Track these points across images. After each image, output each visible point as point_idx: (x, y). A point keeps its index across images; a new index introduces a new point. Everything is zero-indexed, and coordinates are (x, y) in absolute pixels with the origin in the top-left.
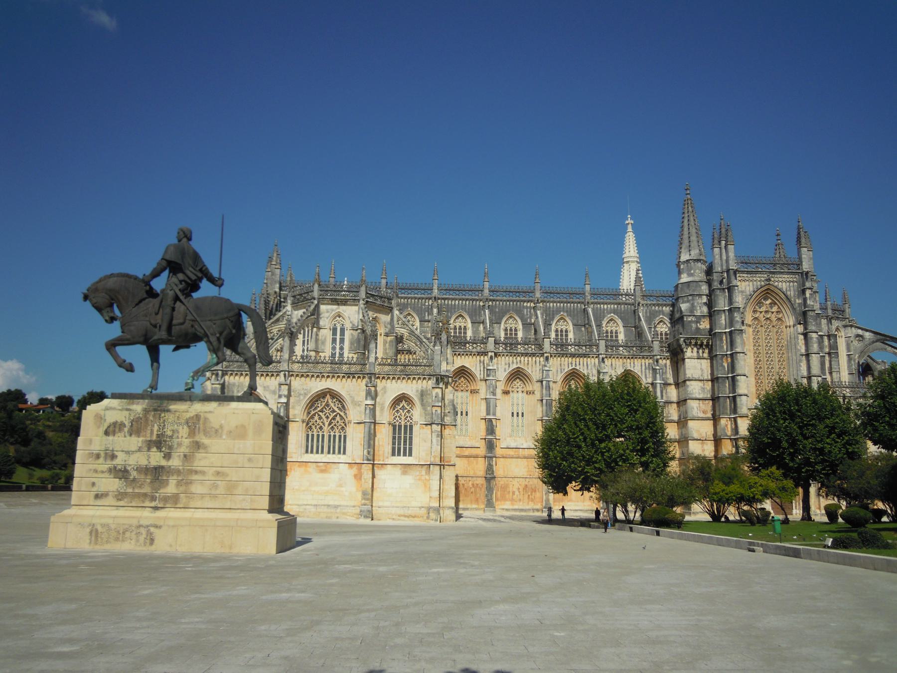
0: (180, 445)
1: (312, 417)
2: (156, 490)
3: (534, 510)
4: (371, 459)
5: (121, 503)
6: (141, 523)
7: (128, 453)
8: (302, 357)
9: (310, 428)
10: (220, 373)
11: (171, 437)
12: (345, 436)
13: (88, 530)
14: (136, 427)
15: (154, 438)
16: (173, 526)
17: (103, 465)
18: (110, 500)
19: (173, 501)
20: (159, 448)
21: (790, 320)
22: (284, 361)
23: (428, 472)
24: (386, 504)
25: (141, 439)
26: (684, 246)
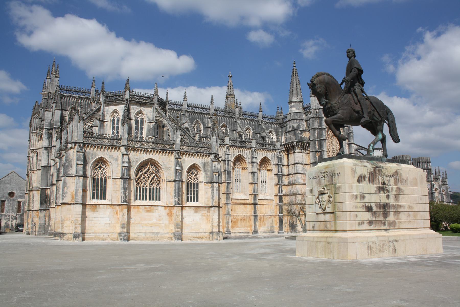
1: (140, 177)
5: (372, 227)
6: (390, 239)
9: (138, 184)
10: (82, 144)
11: (388, 185)
12: (160, 189)
13: (366, 246)
14: (372, 178)
16: (403, 240)
18: (366, 226)
19: (393, 225)
20: (383, 191)
22: (124, 139)
23: (209, 212)
24: (187, 231)
25: (375, 185)
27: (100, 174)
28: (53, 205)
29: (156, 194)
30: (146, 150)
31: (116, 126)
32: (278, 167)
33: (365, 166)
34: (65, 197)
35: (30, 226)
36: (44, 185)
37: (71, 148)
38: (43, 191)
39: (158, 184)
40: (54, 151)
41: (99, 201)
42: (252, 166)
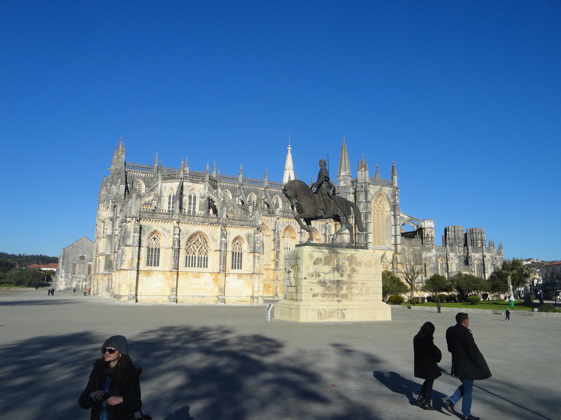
0: (346, 270)
2: (338, 291)
3: (269, 297)
4: (223, 270)
5: (324, 299)
7: (325, 273)
8: (169, 211)
9: (188, 253)
12: (207, 258)
14: (327, 261)
15: (335, 266)
17: (315, 280)
18: (319, 298)
19: (346, 296)
20: (338, 271)
21: (388, 208)
22: (176, 214)
23: (251, 278)
25: (330, 267)
26: (342, 168)
27: (154, 244)
28: (115, 270)
29: (203, 262)
30: (196, 223)
31: (171, 201)
32: (326, 237)
33: (322, 252)
34: (123, 264)
35: (95, 288)
36: (109, 251)
37: (129, 222)
38: (107, 257)
39: (206, 254)
40: (118, 223)
41: (153, 268)
42: (301, 235)
